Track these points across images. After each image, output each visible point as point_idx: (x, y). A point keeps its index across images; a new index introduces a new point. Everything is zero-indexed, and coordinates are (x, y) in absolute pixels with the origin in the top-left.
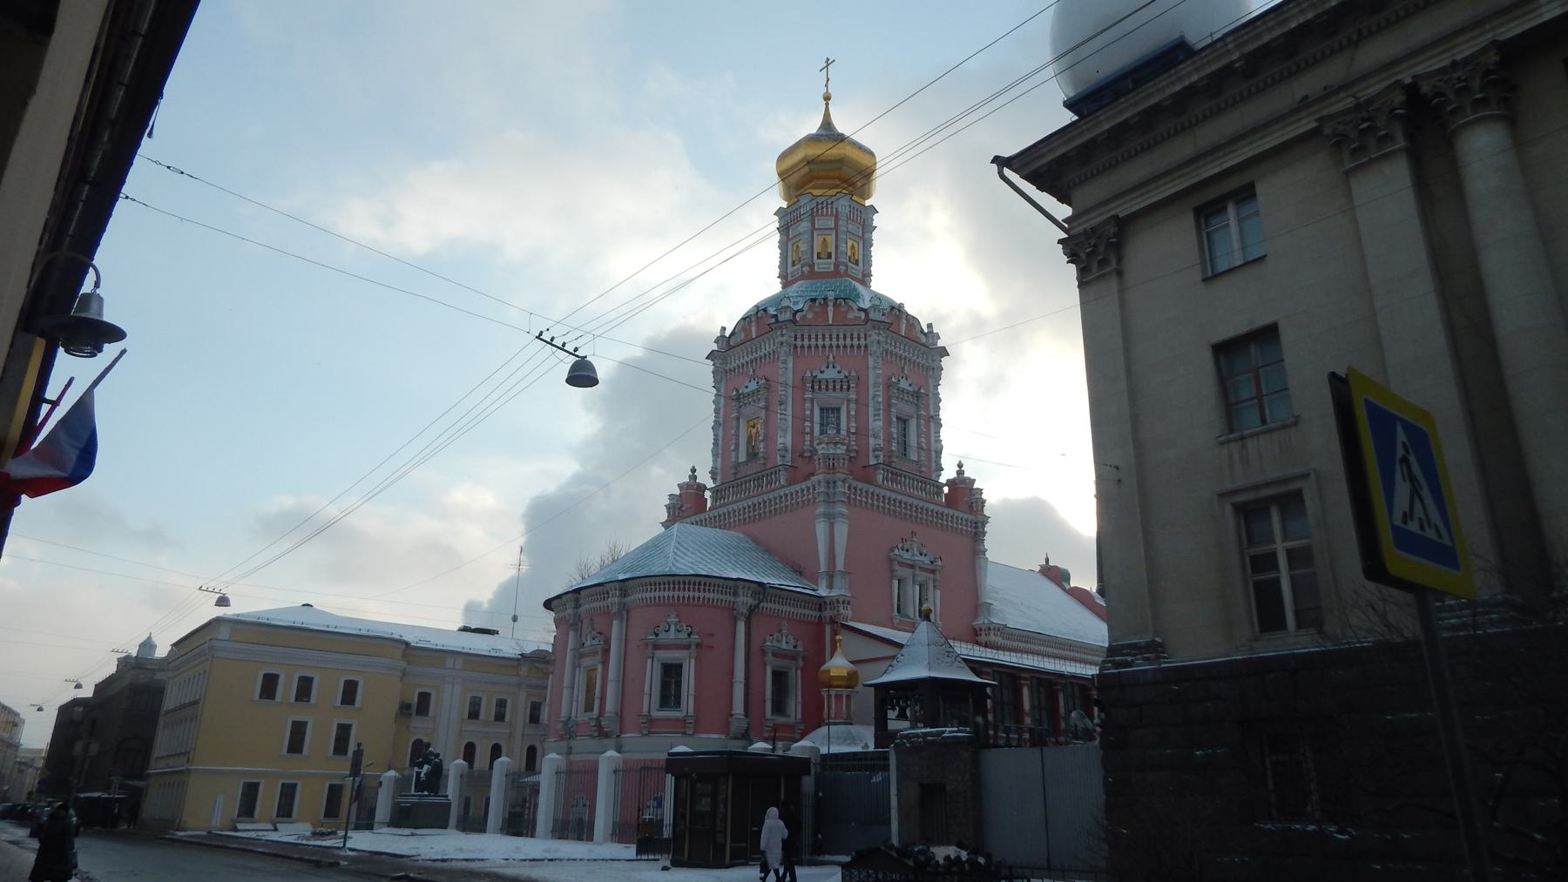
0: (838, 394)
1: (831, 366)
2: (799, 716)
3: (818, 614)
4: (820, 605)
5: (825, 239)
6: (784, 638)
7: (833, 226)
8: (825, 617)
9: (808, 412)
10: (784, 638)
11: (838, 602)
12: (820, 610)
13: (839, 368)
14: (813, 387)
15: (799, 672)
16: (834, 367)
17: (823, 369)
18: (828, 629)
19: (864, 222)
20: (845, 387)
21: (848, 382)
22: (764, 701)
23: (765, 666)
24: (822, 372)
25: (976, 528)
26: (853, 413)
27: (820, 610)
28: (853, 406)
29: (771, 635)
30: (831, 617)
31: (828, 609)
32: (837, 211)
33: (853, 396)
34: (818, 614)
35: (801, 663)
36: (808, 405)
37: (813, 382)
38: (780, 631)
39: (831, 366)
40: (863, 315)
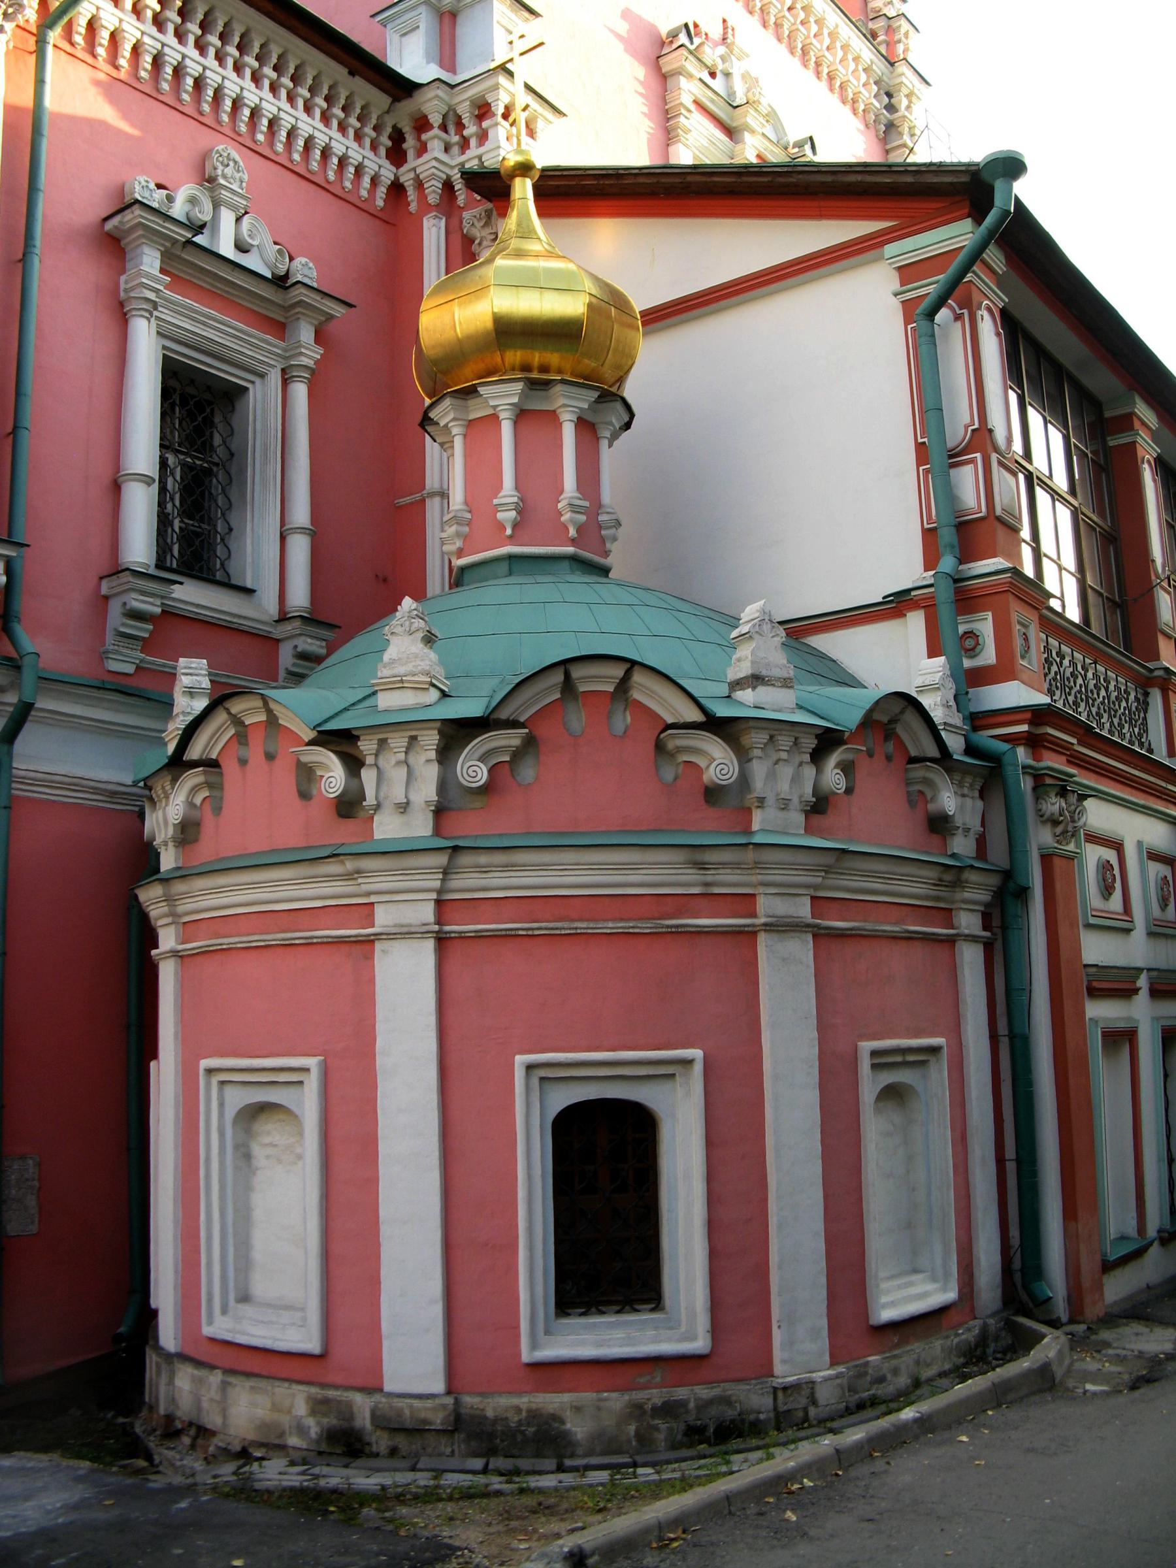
2: (299, 596)
3: (388, 173)
4: (398, 137)
6: (227, 218)
8: (419, 185)
10: (227, 218)
11: (483, 110)
12: (397, 156)
15: (300, 391)
18: (433, 232)
22: (116, 488)
23: (122, 318)
25: (891, 108)
27: (397, 156)
29: (160, 186)
30: (448, 186)
31: (435, 148)
34: (388, 173)
35: (310, 354)
38: (209, 181)
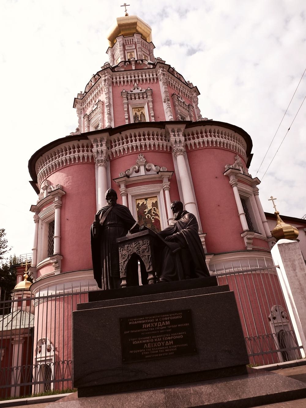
0: (141, 101)
1: (136, 89)
5: (131, 54)
7: (134, 48)
9: (126, 109)
13: (140, 89)
14: (127, 98)
16: (138, 89)
17: (132, 90)
19: (149, 49)
20: (145, 96)
21: (146, 94)
24: (132, 91)
26: (151, 107)
28: (151, 104)
32: (135, 42)
33: (150, 99)
36: (126, 106)
37: (127, 96)
39: (136, 89)
40: (152, 67)
